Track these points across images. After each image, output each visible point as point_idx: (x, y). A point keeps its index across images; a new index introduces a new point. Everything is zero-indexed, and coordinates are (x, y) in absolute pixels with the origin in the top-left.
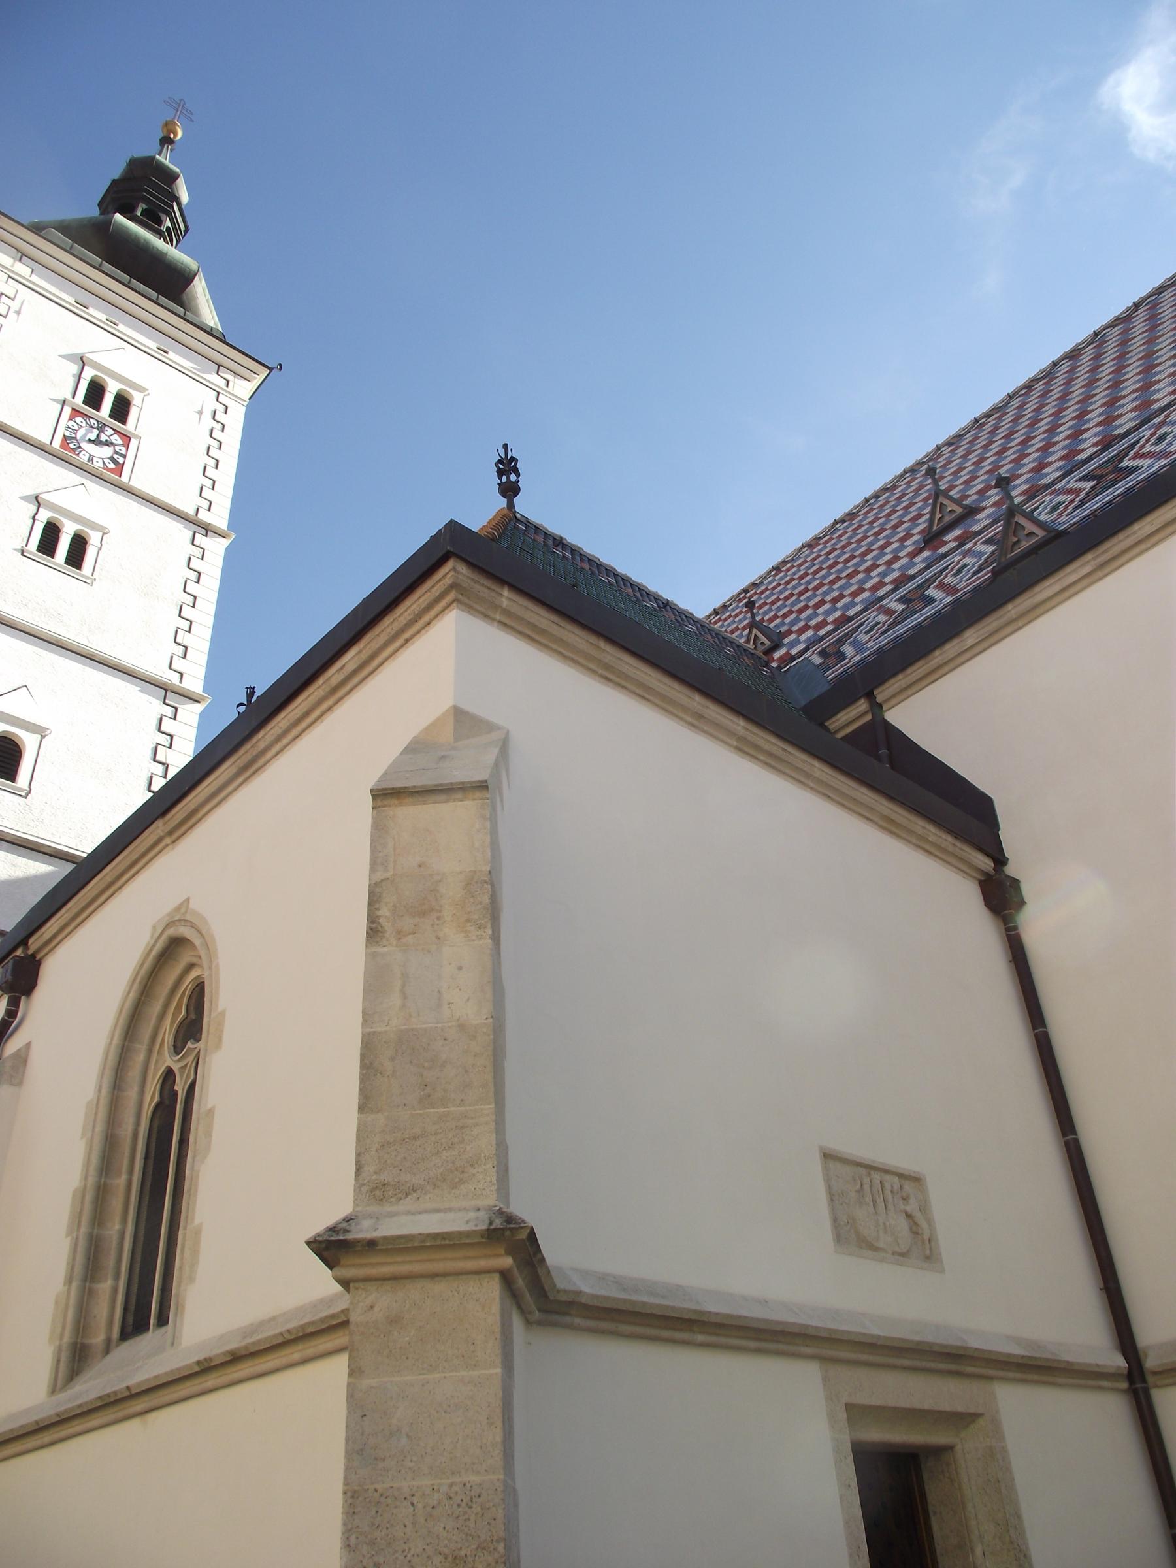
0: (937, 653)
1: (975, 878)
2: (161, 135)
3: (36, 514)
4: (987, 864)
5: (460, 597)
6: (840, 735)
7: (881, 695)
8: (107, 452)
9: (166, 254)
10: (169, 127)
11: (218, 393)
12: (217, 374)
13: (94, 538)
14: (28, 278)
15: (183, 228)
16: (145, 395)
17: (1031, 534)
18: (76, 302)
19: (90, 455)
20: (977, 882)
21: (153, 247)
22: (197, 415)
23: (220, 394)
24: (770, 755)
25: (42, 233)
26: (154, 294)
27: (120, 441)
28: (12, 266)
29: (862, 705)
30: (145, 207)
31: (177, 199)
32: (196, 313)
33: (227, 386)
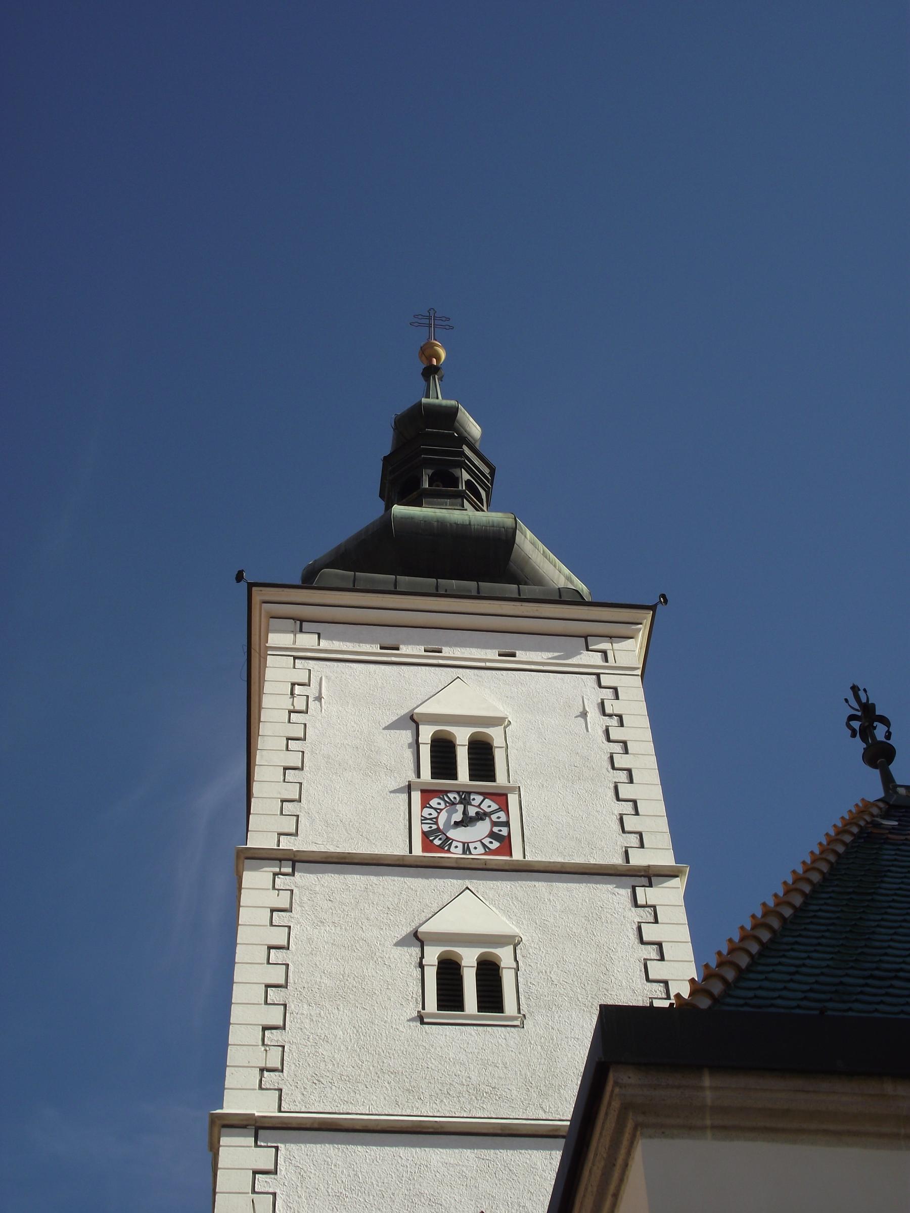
3: (422, 957)
5: (640, 1119)
8: (482, 828)
10: (427, 352)
11: (598, 675)
12: (588, 650)
15: (486, 471)
16: (505, 728)
18: (381, 648)
19: (464, 843)
21: (451, 524)
22: (582, 720)
26: (472, 585)
27: (495, 806)
28: (295, 642)
30: (430, 472)
31: (464, 439)
32: (536, 579)
33: (606, 661)
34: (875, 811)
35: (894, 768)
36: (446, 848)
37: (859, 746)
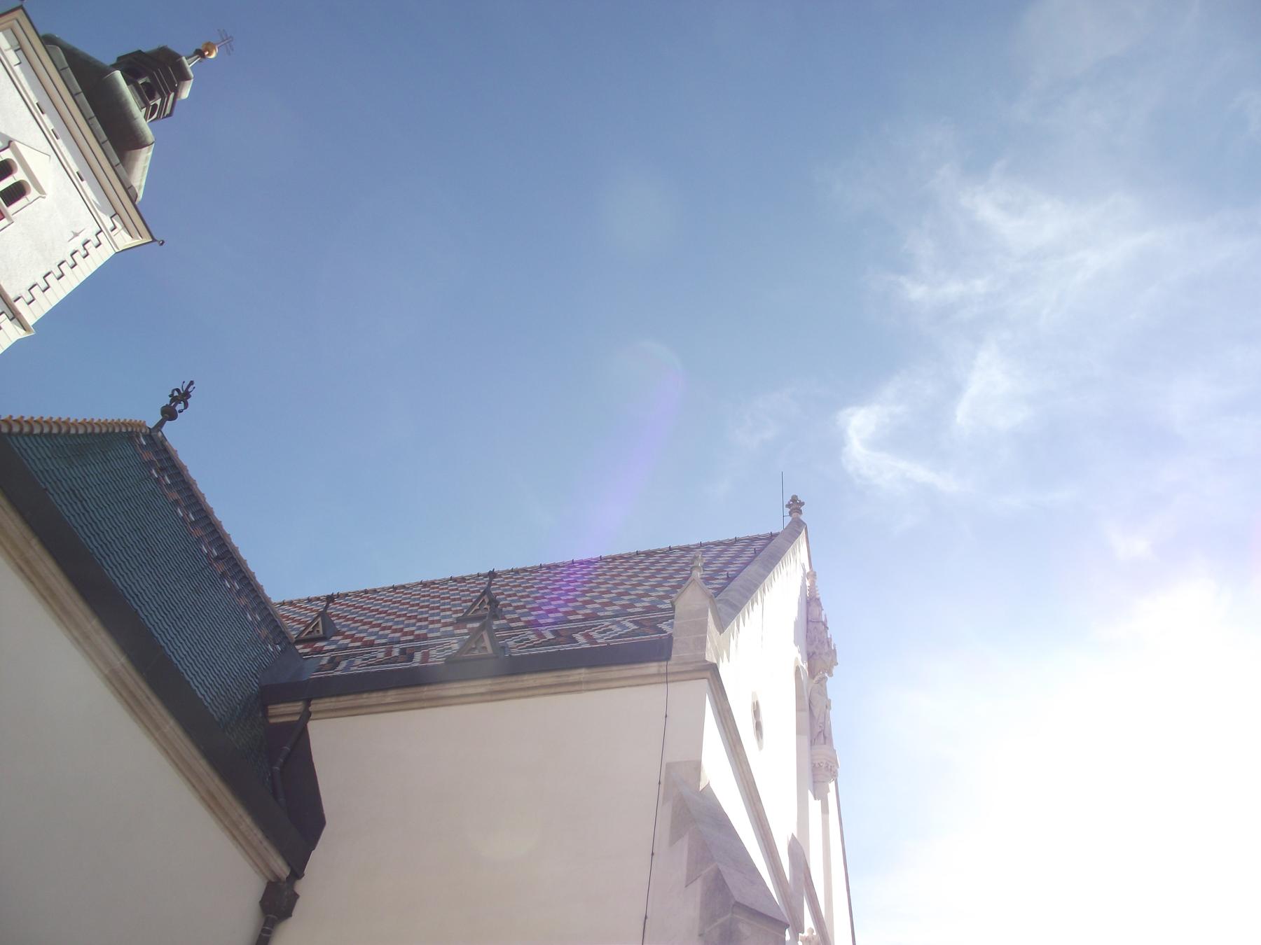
0: (365, 695)
1: (267, 878)
4: (283, 870)
6: (272, 721)
7: (316, 705)
9: (135, 119)
11: (101, 231)
12: (111, 218)
14: (13, 66)
16: (40, 197)
17: (485, 648)
18: (37, 104)
20: (266, 881)
23: (102, 233)
24: (134, 696)
25: (46, 46)
26: (104, 137)
29: (298, 707)
32: (129, 170)
33: (112, 230)
34: (143, 431)
35: (168, 425)
37: (167, 401)
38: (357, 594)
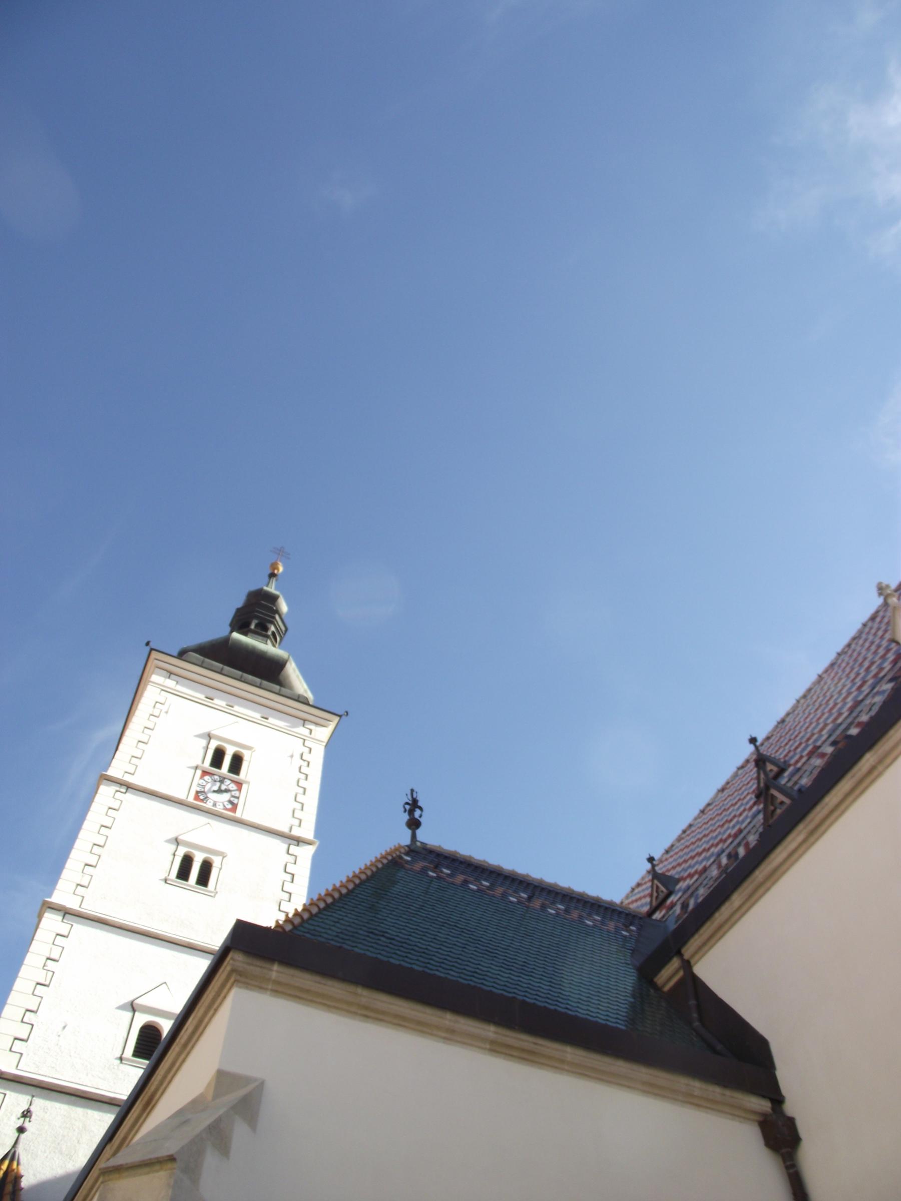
0: (717, 915)
1: (753, 1120)
2: (270, 571)
3: (176, 851)
4: (764, 1105)
5: (238, 978)
6: (666, 989)
7: (688, 951)
8: (226, 797)
11: (304, 740)
13: (216, 861)
15: (283, 628)
17: (782, 803)
20: (756, 1124)
22: (290, 758)
23: (306, 742)
24: (523, 1050)
26: (258, 680)
29: (675, 963)
31: (277, 612)
32: (290, 687)
33: (311, 733)
34: (403, 850)
35: (419, 832)
36: (205, 801)
37: (406, 817)
38: (679, 839)
